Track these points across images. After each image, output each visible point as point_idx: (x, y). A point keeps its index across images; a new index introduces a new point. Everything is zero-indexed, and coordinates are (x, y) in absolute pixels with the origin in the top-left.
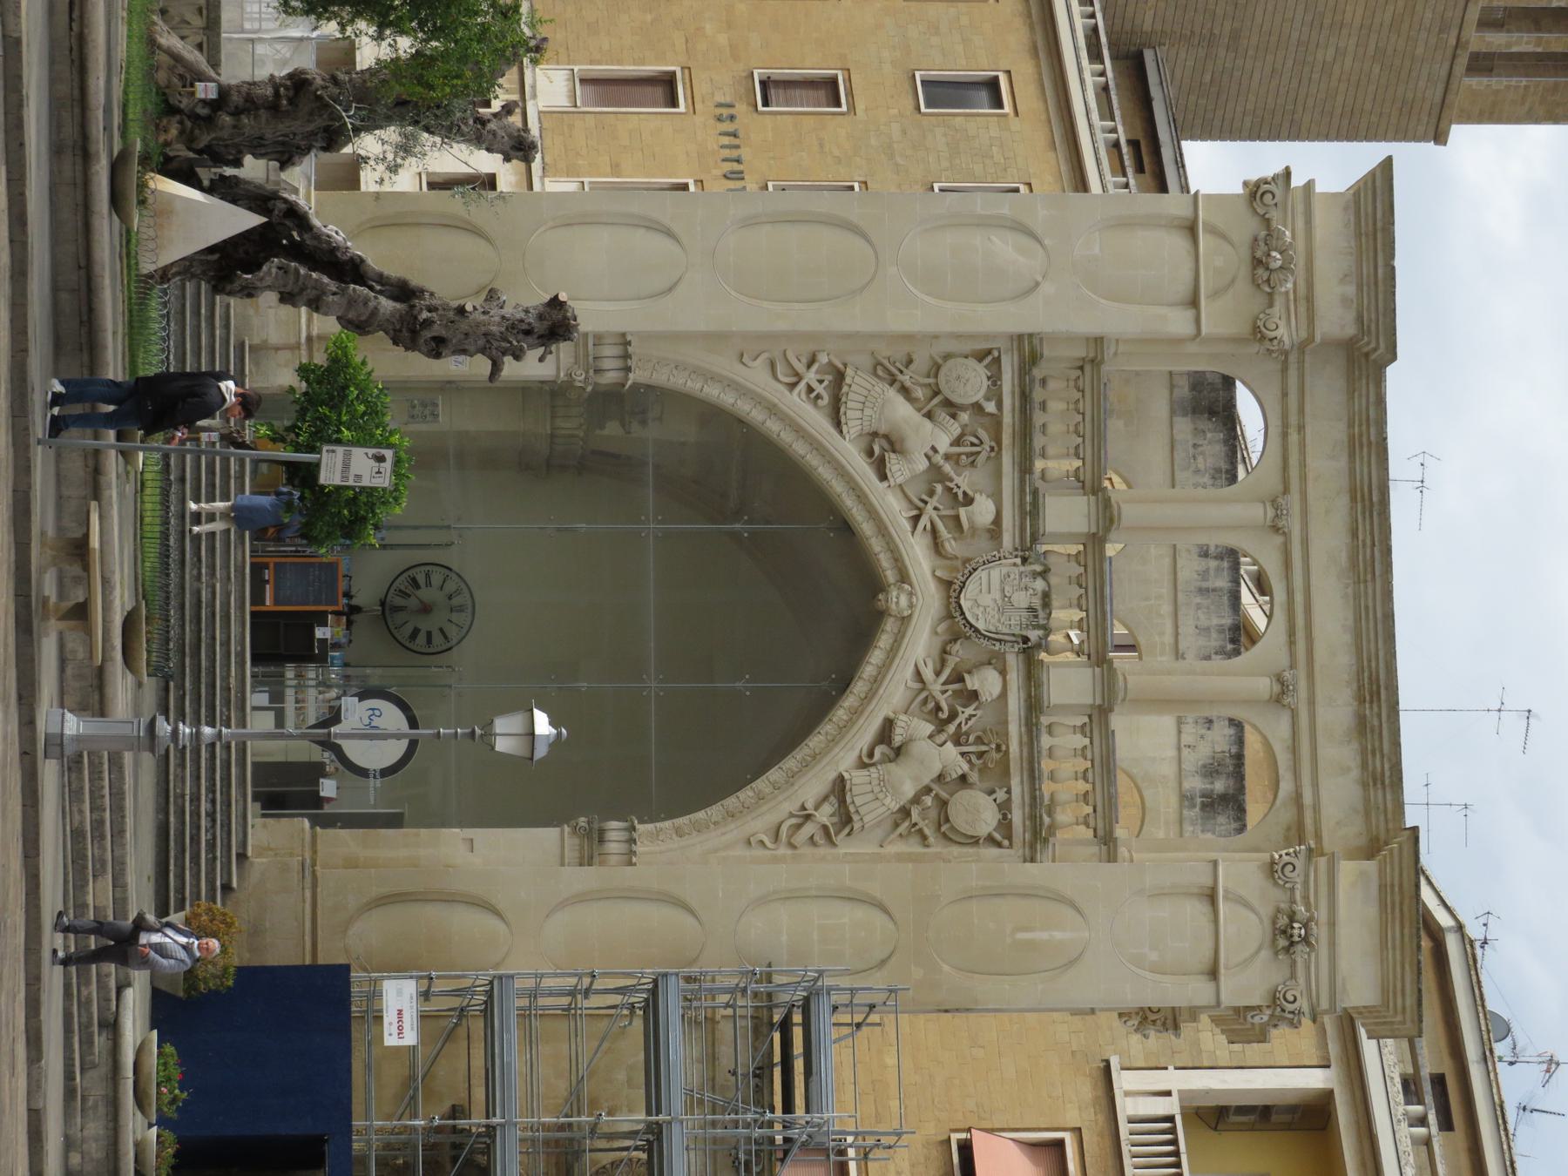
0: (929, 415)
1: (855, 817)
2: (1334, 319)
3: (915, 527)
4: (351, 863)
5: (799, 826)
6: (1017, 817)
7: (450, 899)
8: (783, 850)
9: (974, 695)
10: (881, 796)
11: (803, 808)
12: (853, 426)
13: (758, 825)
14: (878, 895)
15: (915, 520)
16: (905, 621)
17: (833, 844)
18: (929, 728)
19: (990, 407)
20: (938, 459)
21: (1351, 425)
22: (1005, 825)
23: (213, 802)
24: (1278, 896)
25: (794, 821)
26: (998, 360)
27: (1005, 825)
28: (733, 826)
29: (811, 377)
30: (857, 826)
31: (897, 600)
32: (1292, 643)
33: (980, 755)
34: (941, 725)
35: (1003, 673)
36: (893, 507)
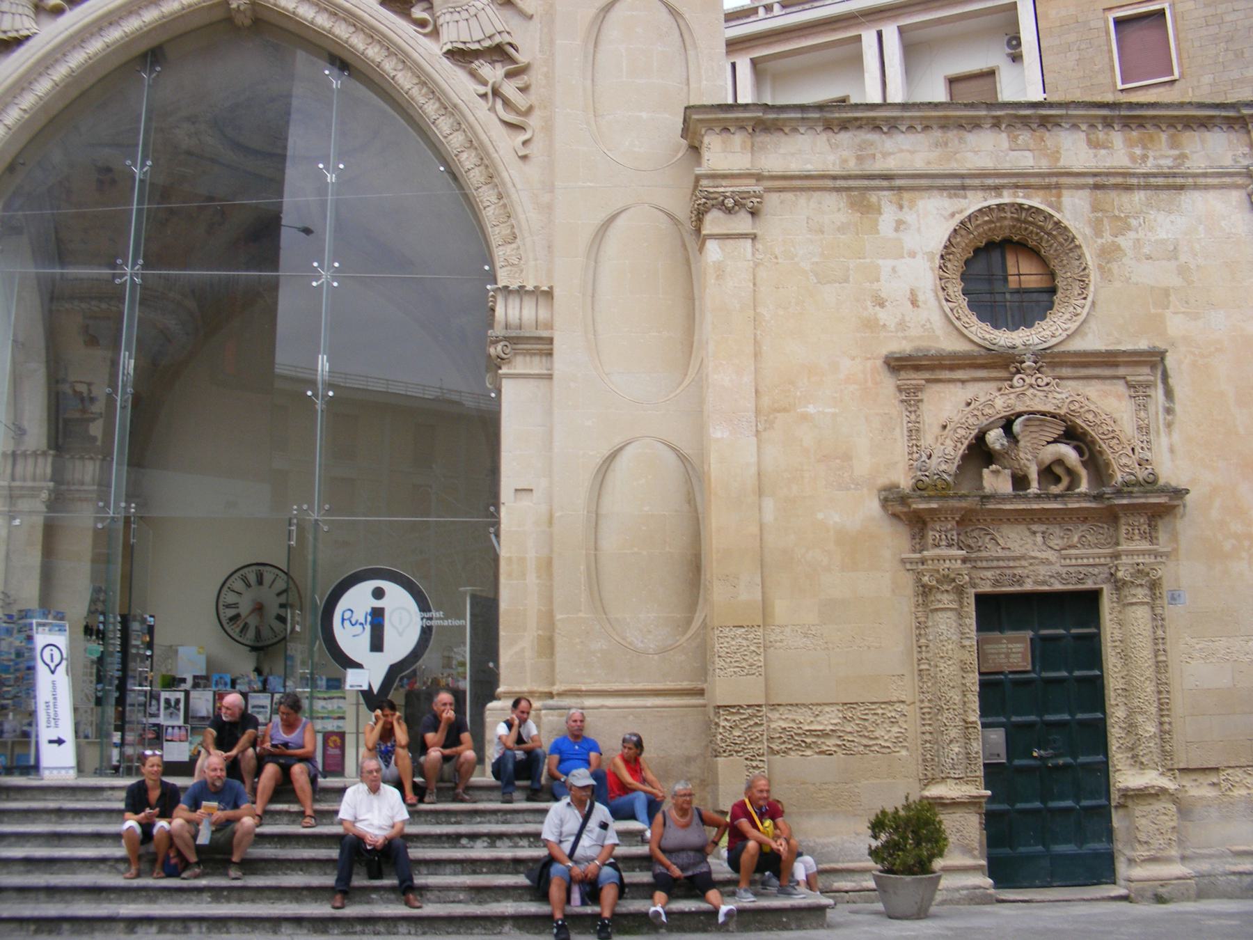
1: (497, 39)
4: (548, 646)
5: (507, 103)
7: (596, 519)
8: (534, 121)
10: (472, 11)
11: (484, 96)
13: (504, 144)
14: (592, 12)
23: (473, 837)
25: (499, 105)
28: (505, 175)
30: (507, 38)
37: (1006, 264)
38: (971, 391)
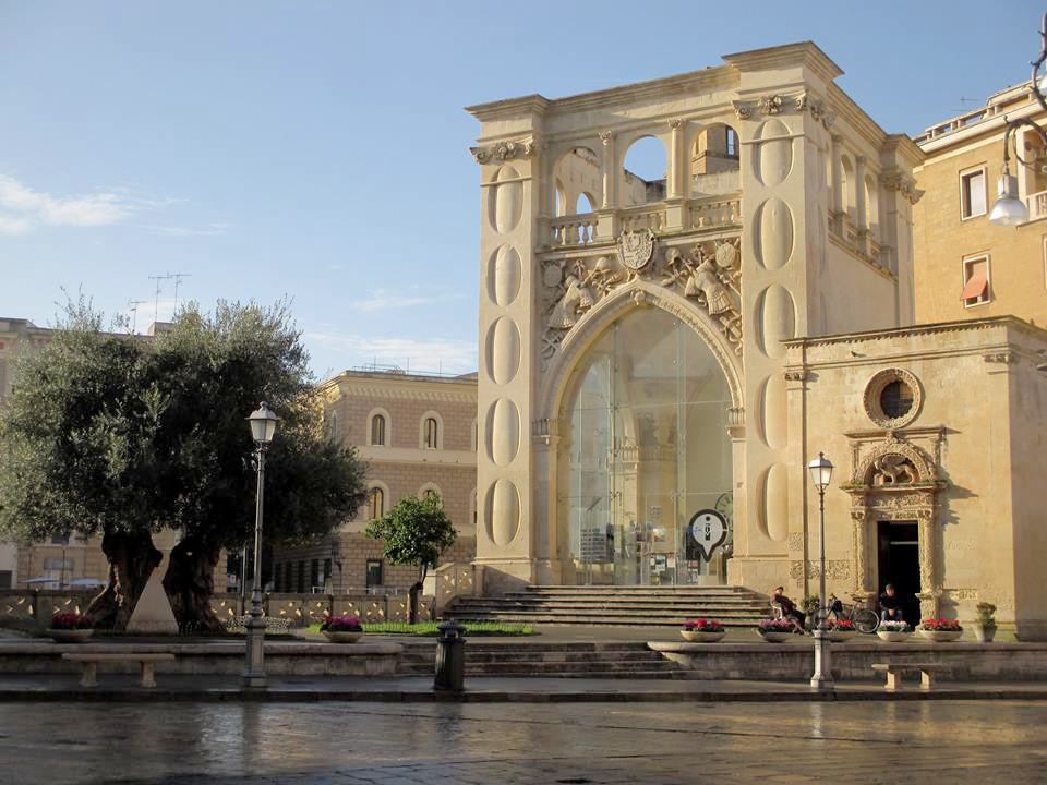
9: (677, 260)
17: (739, 319)
18: (690, 278)
19: (563, 264)
20: (582, 284)
21: (574, 112)
22: (732, 241)
26: (546, 262)
27: (732, 241)
29: (550, 342)
33: (703, 255)
34: (690, 274)
37: (889, 396)
38: (876, 444)
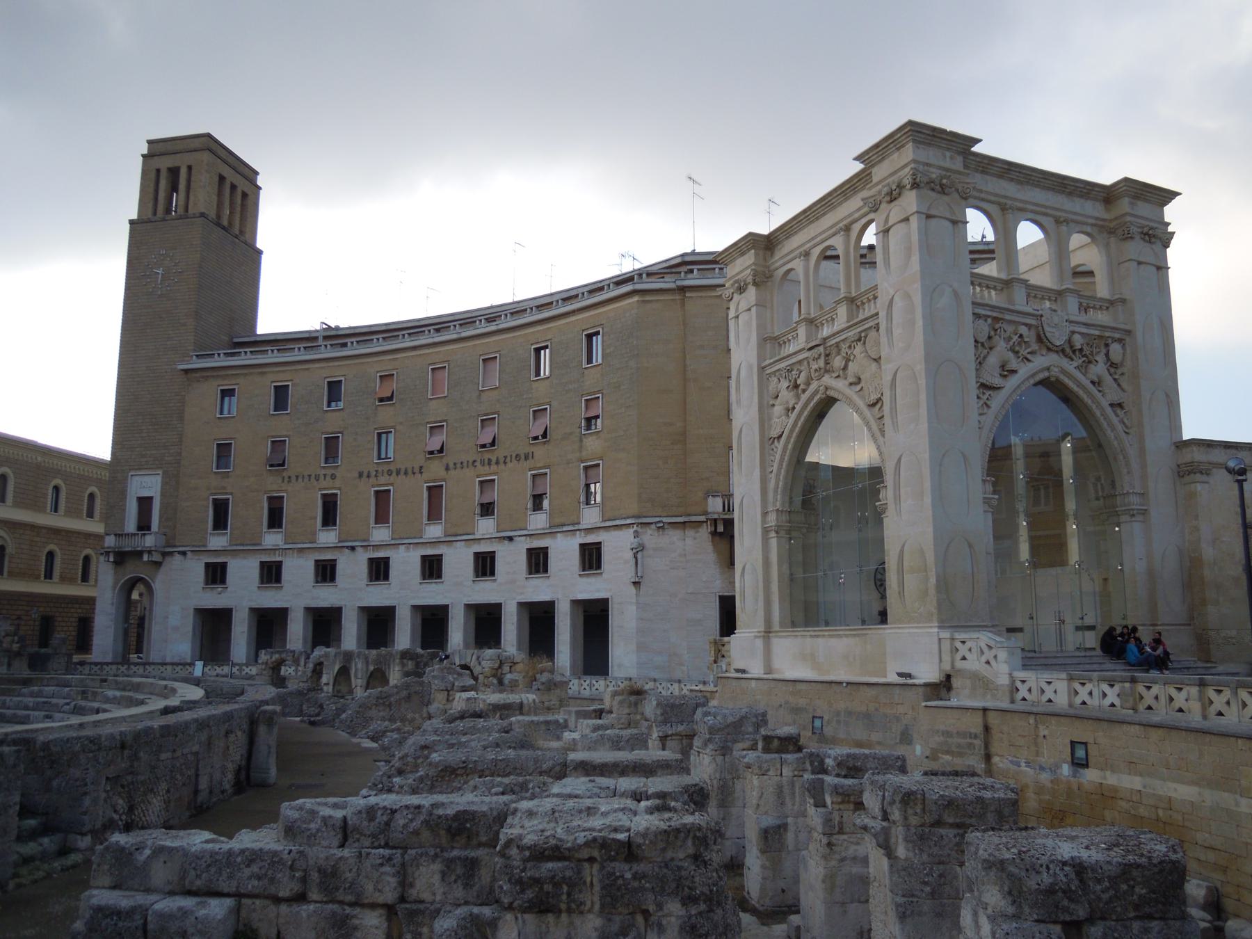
0: (991, 349)
2: (958, 164)
3: (1028, 360)
6: (1117, 336)
12: (997, 381)
15: (1028, 360)
16: (1063, 371)
18: (1092, 366)
21: (977, 171)
24: (1138, 237)
27: (1120, 341)
31: (1055, 372)
32: (1046, 214)
34: (1090, 362)
35: (1073, 332)
36: (1024, 370)
